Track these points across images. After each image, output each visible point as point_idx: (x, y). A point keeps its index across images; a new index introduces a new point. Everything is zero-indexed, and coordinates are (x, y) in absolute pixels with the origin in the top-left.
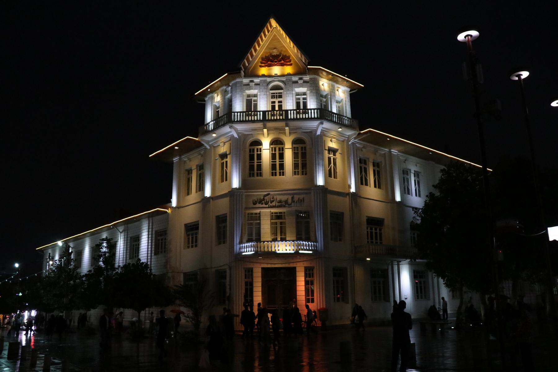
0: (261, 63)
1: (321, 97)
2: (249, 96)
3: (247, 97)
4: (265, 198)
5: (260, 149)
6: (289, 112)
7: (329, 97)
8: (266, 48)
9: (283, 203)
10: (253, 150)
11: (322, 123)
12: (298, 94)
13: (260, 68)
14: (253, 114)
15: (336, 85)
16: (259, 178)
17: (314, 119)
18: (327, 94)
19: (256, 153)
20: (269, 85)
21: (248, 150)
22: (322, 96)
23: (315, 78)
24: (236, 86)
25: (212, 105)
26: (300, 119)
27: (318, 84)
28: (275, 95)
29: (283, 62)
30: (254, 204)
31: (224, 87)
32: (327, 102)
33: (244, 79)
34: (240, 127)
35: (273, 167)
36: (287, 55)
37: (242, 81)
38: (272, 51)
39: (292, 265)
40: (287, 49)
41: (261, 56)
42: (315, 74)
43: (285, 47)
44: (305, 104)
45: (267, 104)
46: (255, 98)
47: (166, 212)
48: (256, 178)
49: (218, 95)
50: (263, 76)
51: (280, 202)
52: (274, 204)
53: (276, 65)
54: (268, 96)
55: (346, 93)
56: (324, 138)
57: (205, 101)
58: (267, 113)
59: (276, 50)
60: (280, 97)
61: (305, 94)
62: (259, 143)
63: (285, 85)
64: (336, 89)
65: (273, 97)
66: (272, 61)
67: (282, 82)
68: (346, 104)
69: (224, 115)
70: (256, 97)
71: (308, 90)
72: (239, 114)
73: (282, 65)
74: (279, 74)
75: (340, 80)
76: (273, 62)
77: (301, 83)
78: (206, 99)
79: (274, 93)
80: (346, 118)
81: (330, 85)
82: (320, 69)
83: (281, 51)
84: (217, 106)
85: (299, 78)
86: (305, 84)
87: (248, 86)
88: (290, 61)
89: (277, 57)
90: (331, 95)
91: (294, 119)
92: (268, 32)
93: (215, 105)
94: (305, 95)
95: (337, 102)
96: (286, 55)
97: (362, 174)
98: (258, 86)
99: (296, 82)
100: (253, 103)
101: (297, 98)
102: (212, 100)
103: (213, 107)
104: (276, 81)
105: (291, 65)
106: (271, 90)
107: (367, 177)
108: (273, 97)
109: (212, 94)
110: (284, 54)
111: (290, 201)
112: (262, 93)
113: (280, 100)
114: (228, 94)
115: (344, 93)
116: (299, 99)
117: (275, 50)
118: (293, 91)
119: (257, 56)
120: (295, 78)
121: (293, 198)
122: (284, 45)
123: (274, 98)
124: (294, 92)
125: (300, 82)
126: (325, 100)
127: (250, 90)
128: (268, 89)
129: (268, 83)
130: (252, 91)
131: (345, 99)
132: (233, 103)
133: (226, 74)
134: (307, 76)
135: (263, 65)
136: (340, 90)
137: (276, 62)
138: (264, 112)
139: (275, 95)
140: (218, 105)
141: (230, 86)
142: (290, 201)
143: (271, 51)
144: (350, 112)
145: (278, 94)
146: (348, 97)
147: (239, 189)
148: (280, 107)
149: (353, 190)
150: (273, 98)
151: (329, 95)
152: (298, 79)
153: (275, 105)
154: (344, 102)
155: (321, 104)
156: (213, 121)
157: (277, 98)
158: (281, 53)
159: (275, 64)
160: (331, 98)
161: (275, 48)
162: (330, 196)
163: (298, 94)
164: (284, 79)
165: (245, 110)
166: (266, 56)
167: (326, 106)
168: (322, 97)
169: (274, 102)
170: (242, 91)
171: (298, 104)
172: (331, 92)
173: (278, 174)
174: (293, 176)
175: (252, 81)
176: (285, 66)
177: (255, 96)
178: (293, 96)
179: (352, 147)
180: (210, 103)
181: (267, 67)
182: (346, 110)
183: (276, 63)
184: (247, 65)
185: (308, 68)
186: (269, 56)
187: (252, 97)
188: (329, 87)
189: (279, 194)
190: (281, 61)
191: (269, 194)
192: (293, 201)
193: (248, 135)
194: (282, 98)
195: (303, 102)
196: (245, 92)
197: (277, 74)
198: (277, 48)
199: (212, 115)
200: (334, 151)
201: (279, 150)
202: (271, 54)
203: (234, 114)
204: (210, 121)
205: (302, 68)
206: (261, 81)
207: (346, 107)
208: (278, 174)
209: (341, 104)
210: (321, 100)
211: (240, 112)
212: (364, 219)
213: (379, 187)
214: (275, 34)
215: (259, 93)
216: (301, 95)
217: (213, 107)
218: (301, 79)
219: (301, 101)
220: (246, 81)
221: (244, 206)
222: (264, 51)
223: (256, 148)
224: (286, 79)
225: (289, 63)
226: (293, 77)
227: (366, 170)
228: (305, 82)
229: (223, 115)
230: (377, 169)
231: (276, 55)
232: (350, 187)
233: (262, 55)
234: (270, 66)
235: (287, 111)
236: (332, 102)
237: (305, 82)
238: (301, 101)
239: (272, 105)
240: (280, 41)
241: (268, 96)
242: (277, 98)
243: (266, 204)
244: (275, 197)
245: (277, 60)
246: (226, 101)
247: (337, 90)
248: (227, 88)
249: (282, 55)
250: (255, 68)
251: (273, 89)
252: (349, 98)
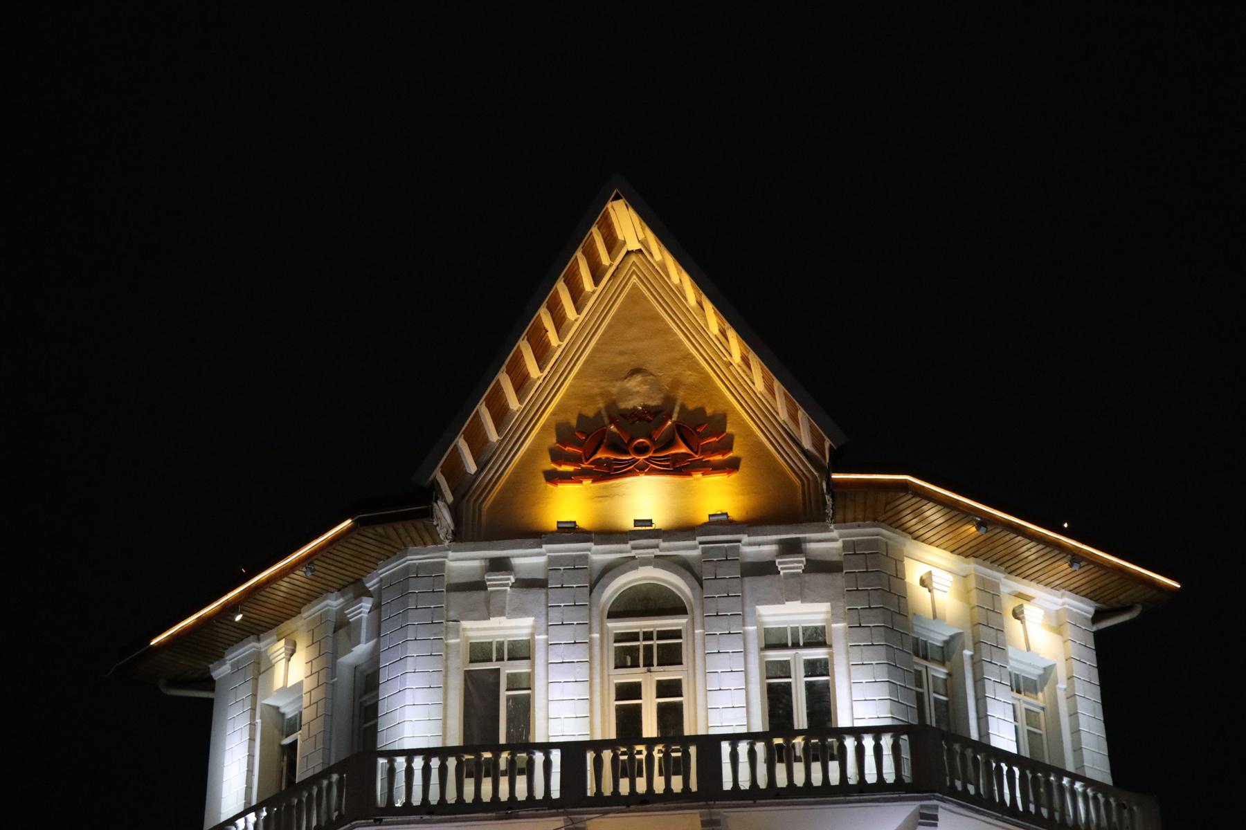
1: (917, 655)
2: (480, 652)
3: (471, 662)
6: (726, 747)
7: (968, 653)
8: (579, 373)
11: (923, 816)
12: (773, 641)
13: (550, 486)
14: (503, 765)
15: (1009, 585)
17: (880, 791)
18: (952, 638)
20: (605, 586)
22: (921, 650)
23: (873, 544)
24: (405, 594)
25: (253, 709)
26: (792, 792)
27: (899, 576)
28: (641, 643)
29: (683, 450)
31: (333, 603)
32: (952, 685)
33: (450, 554)
36: (709, 411)
37: (443, 564)
38: (619, 384)
40: (708, 377)
41: (553, 414)
42: (876, 521)
43: (697, 363)
44: (820, 700)
45: (591, 701)
46: (520, 667)
49: (295, 645)
50: (569, 532)
53: (641, 469)
54: (597, 649)
55: (1069, 631)
57: (209, 684)
58: (590, 756)
59: (644, 382)
60: (671, 656)
61: (816, 638)
63: (696, 584)
64: (1009, 605)
65: (625, 658)
66: (618, 448)
68: (1071, 697)
69: (326, 773)
70: (528, 658)
71: (835, 617)
72: (418, 763)
73: (679, 468)
74: (659, 522)
75: (1030, 551)
76: (627, 453)
77: (793, 575)
78: (220, 672)
79: (634, 637)
80: (1078, 786)
81: (972, 583)
82: (905, 486)
83: (676, 384)
84: (283, 715)
85: (780, 542)
86: (820, 578)
87: (478, 596)
88: (727, 446)
89: (648, 418)
90: (977, 644)
91: (754, 795)
92: (597, 275)
93: (277, 708)
94: (823, 644)
95: (1020, 685)
96: (701, 410)
98: (539, 594)
99: (764, 569)
100: (509, 698)
101: (768, 662)
102: (256, 679)
103: (258, 721)
104: (645, 562)
105: (731, 466)
106: (614, 614)
108: (625, 658)
109: (259, 640)
110: (691, 406)
112: (566, 635)
114: (359, 643)
115: (1058, 630)
116: (784, 668)
117: (639, 378)
118: (748, 619)
120: (758, 547)
122: (690, 356)
123: (635, 665)
124: (751, 629)
125: (792, 565)
126: (940, 672)
127: (487, 618)
128: (595, 611)
129: (595, 577)
130: (495, 622)
131: (1070, 670)
132: (384, 692)
133: (348, 523)
134: (827, 530)
135: (570, 468)
136: (1029, 610)
137: (641, 450)
138: (573, 752)
139: (637, 648)
140: (290, 712)
141: (368, 594)
143: (615, 388)
144: (1104, 744)
145: (655, 643)
146: (1084, 651)
148: (670, 716)
150: (625, 666)
151: (969, 641)
152: (774, 548)
153: (639, 707)
154: (1062, 685)
155: (920, 698)
156: (256, 809)
157: (648, 664)
158: (669, 400)
159: (634, 461)
160: (977, 663)
161: (636, 371)
163: (774, 641)
164: (690, 550)
165: (455, 740)
166: (581, 417)
167: (951, 711)
168: (925, 658)
169: (630, 691)
170: (440, 623)
171: (778, 698)
172: (975, 625)
175: (500, 565)
176: (698, 475)
177: (520, 651)
178: (745, 653)
180: (244, 694)
181: (587, 482)
182: (1076, 732)
183: (642, 458)
184: (472, 468)
185: (833, 485)
186: (599, 414)
187: (500, 659)
188: (964, 594)
190: (670, 444)
194: (681, 663)
195: (809, 686)
196: (457, 633)
197: (649, 522)
198: (651, 369)
199: (250, 771)
202: (611, 406)
203: (391, 762)
204: (241, 809)
205: (797, 482)
206: (552, 560)
207: (1074, 714)
209: (1041, 699)
210: (918, 675)
211: (427, 753)
214: (635, 287)
215: (540, 638)
216: (796, 645)
217: (258, 721)
218: (792, 548)
219: (799, 684)
222: (571, 385)
224: (704, 551)
225: (719, 458)
226: (745, 538)
229: (318, 770)
231: (645, 407)
233: (560, 409)
235: (709, 745)
236: (989, 686)
237: (817, 566)
238: (799, 684)
239: (619, 709)
240: (669, 331)
241: (597, 649)
242: (648, 664)
245: (650, 437)
246: (345, 678)
247: (1017, 614)
248: (347, 605)
249: (677, 409)
250: (519, 487)
251: (619, 611)
252: (1091, 657)
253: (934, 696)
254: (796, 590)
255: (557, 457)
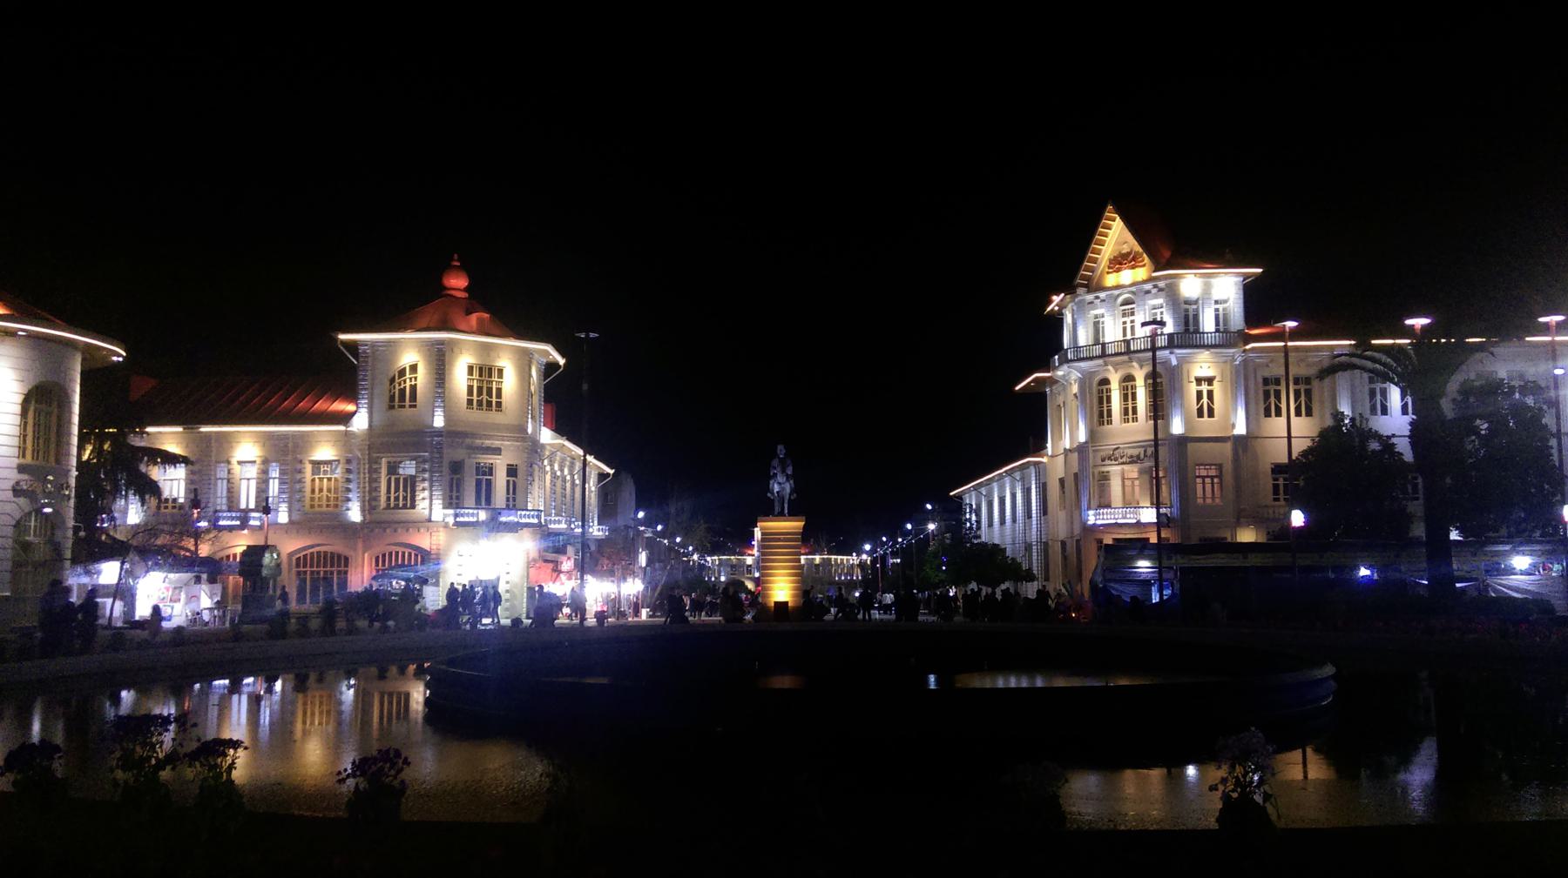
0: (1109, 268)
2: (1096, 317)
4: (1116, 452)
5: (1110, 389)
9: (1135, 459)
10: (1102, 390)
16: (1110, 426)
19: (1105, 394)
21: (1095, 390)
22: (1187, 302)
23: (1171, 284)
30: (1103, 460)
32: (1197, 310)
34: (1082, 364)
35: (1126, 412)
39: (1144, 536)
47: (1042, 462)
48: (1107, 427)
51: (1132, 457)
52: (1124, 460)
56: (1185, 367)
60: (1133, 314)
62: (1105, 382)
66: (1121, 264)
67: (1133, 293)
79: (1125, 310)
89: (1129, 254)
97: (1270, 403)
99: (1148, 292)
105: (1144, 266)
106: (1122, 305)
107: (1280, 403)
108: (1124, 315)
111: (1142, 456)
113: (1132, 318)
119: (1103, 258)
120: (1148, 286)
121: (1145, 451)
124: (1147, 307)
126: (1195, 307)
142: (1142, 456)
143: (1121, 247)
147: (1086, 442)
149: (1240, 429)
158: (1131, 251)
161: (1126, 243)
162: (1190, 446)
164: (1133, 289)
167: (1196, 317)
169: (1125, 323)
173: (1131, 420)
174: (1147, 421)
175: (1097, 298)
179: (1242, 367)
189: (1129, 447)
190: (1131, 262)
191: (1117, 448)
192: (1145, 456)
193: (1094, 372)
200: (1210, 381)
201: (1132, 389)
208: (1131, 420)
210: (1187, 310)
212: (1268, 469)
213: (1309, 413)
220: (1090, 297)
221: (1091, 465)
223: (1104, 387)
227: (1278, 395)
228: (1161, 290)
230: (1302, 388)
232: (1233, 426)
234: (1118, 271)
237: (1161, 290)
243: (1116, 459)
244: (1126, 451)
251: (1123, 304)
252: (1241, 292)
253: (1191, 314)
254: (1156, 297)
255: (1109, 268)
